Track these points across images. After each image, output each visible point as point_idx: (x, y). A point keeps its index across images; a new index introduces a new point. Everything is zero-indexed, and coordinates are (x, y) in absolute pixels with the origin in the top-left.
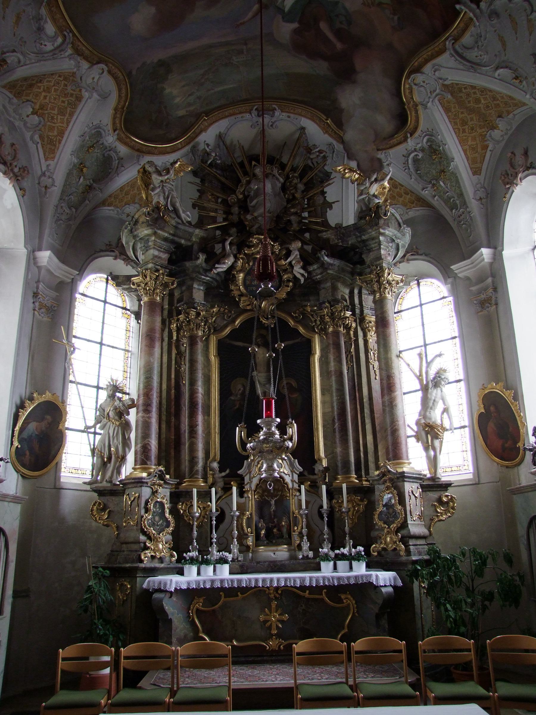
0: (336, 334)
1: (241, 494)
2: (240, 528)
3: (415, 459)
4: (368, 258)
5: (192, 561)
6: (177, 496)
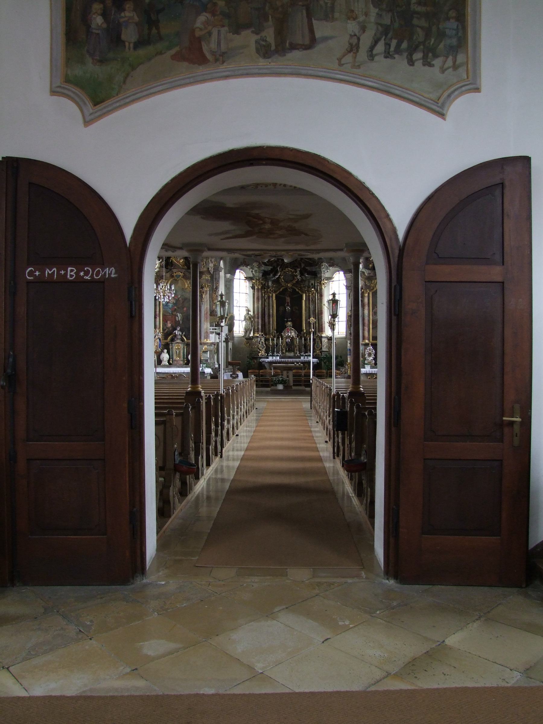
0: (309, 296)
1: (282, 339)
2: (282, 348)
3: (328, 332)
4: (319, 276)
5: (271, 356)
6: (266, 340)
